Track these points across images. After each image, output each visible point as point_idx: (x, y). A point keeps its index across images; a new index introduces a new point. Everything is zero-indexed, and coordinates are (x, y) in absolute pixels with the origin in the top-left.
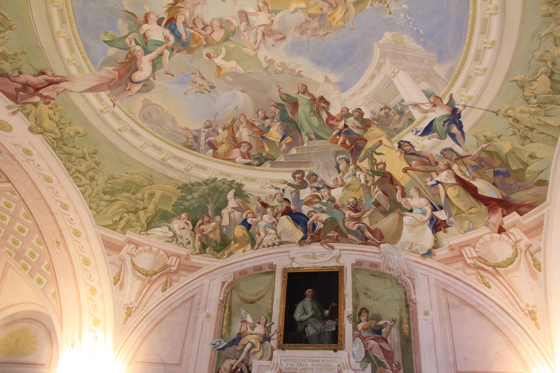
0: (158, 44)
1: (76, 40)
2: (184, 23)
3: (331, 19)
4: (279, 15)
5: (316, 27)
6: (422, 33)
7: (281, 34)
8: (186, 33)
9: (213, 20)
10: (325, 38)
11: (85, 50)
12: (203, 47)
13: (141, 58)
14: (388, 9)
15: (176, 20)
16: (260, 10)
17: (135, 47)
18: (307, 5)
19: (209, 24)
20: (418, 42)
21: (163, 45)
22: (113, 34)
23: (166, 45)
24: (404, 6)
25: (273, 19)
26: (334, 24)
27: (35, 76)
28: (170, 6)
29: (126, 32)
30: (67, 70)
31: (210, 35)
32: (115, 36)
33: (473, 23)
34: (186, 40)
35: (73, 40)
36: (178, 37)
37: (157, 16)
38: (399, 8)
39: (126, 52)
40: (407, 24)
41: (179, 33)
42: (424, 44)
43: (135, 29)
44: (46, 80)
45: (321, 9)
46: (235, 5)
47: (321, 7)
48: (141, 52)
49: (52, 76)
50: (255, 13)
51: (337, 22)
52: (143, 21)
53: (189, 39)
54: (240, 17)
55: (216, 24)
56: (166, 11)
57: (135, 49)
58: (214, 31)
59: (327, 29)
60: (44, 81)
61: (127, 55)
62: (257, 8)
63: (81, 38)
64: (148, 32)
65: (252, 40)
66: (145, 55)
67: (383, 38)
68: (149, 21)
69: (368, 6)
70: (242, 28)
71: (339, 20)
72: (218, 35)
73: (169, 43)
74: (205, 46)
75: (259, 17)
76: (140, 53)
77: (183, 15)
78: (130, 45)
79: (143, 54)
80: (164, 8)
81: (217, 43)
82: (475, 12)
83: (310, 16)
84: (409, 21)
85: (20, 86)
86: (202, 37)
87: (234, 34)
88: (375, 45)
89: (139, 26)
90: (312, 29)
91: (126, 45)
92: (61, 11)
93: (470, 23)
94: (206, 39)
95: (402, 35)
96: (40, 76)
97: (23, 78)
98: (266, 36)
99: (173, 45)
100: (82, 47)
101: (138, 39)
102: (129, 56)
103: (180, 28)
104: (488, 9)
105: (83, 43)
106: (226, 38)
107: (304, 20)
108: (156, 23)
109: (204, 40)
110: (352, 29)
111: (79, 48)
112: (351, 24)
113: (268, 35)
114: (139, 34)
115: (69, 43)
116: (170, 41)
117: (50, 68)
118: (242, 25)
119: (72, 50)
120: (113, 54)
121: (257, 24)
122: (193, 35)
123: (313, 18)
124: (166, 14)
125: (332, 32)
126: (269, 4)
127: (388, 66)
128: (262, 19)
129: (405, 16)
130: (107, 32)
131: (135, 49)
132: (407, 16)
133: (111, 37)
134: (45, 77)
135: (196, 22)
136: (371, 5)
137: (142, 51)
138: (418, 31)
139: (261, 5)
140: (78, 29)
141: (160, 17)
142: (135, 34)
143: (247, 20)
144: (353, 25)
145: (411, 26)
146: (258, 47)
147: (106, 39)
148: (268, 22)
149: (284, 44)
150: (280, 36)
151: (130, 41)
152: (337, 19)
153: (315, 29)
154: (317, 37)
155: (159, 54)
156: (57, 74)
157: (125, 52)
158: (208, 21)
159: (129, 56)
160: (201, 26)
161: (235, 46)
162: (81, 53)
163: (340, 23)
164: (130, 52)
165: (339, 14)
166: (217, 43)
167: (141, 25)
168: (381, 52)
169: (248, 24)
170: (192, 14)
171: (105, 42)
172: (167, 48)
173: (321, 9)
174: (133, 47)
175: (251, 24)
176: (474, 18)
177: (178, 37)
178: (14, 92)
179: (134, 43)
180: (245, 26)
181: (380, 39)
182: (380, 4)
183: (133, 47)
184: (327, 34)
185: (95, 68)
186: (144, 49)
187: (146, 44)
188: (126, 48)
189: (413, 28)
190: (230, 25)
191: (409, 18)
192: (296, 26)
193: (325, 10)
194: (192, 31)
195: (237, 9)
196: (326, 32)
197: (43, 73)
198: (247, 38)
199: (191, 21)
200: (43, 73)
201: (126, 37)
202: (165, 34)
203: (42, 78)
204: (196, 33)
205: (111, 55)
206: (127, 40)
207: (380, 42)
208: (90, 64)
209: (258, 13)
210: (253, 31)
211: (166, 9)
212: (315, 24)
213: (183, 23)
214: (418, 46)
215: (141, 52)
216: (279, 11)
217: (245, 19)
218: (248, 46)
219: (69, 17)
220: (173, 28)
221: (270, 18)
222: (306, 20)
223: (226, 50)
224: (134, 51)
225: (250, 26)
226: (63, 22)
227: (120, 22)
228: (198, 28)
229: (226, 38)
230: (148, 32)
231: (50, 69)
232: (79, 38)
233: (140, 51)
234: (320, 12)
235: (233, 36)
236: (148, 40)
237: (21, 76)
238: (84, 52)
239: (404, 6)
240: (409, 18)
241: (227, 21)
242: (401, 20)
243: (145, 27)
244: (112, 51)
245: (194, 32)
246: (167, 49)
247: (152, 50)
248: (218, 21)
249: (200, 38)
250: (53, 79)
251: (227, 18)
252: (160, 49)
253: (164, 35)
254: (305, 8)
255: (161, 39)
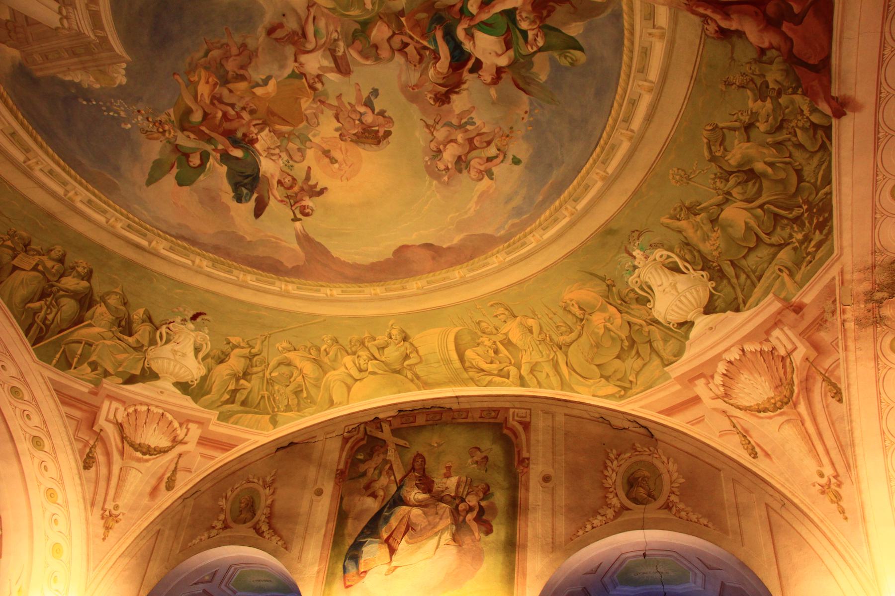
0: (487, 27)
1: (630, 67)
2: (437, 58)
3: (210, 80)
4: (288, 71)
5: (227, 61)
6: (80, 100)
7: (276, 40)
8: (435, 40)
9: (391, 58)
10: (205, 47)
11: (623, 44)
12: (406, 12)
13: (524, 4)
14: (146, 116)
15: (451, 66)
16: (319, 76)
17: (530, 27)
18: (254, 93)
19: (396, 53)
20: (78, 86)
21: (478, 24)
22: (563, 59)
23: (473, 23)
24: (129, 126)
25: (297, 64)
26: (203, 73)
27: (740, 34)
28: (457, 90)
29: (538, 59)
30: (674, 20)
31: (394, 34)
32: (560, 55)
33: (36, 140)
34: (435, 28)
35: (633, 69)
36: (450, 37)
37: (479, 76)
38: (133, 122)
39: (549, 22)
40: (108, 104)
41: (448, 43)
42: (63, 84)
43: (522, 60)
44: (727, 16)
45: (231, 91)
46: (358, 84)
47: (232, 94)
48: (521, 16)
49: (711, 19)
50: (325, 72)
51: (200, 79)
52: (504, 72)
53: (430, 29)
54: (348, 65)
55: (384, 53)
56: (464, 83)
57: (530, 24)
58: (389, 40)
59: (209, 63)
60: (732, 16)
61: (548, 15)
62: (324, 80)
63: (620, 68)
64: (500, 52)
65: (322, 23)
66: (515, 9)
67: (123, 72)
68: (494, 70)
69: (171, 111)
70: (341, 44)
71: (199, 82)
72: (380, 32)
73: (466, 26)
74: (402, 13)
75: (318, 66)
76: (524, 15)
77: (439, 73)
78: (539, 34)
79: (517, 12)
80: (467, 89)
81: (381, 18)
82: (47, 153)
83: (242, 78)
84: (109, 110)
85: (786, 27)
86: (408, 31)
87: (353, 34)
88: (128, 58)
89: (512, 65)
90: (231, 56)
91: (545, 35)
92: (628, 120)
93: (39, 139)
94: (400, 26)
95: (104, 86)
96: (733, 28)
97: (768, 39)
98: (300, 33)
99: (459, 21)
100: (626, 50)
101: (521, 41)
102: (545, 13)
103: (444, 51)
104: (37, 163)
105: (621, 59)
106: (365, 26)
107: (249, 70)
108: (484, 66)
109: (404, 26)
110: (174, 74)
111: (632, 51)
112: (181, 81)
113: (298, 35)
114: (517, 52)
115: (644, 67)
116: (465, 29)
117: (703, 36)
118: (342, 50)
119: (646, 53)
120: (574, 24)
121: (318, 54)
122: (424, 36)
123: (237, 74)
124: (466, 78)
125: (200, 59)
126: (308, 88)
127: (84, 28)
128: (314, 63)
129: (119, 114)
130: (571, 64)
131: (530, 24)
132: (116, 115)
133: (568, 54)
134: (724, 24)
135: (418, 57)
136: (169, 115)
137: (518, 18)
138: (88, 100)
139: (319, 86)
140: (617, 84)
141: (475, 75)
142: (524, 53)
143: (335, 59)
144: (177, 80)
145: (101, 103)
146: (309, 10)
147: (578, 53)
148: (303, 58)
149: (269, 18)
150: (279, 34)
151: (535, 40)
152: (203, 81)
153: (227, 58)
154: (219, 45)
155: (489, 6)
156: (697, 20)
157: (549, 22)
158: (399, 58)
159: (545, 13)
160: (410, 49)
161: (348, 11)
162: (632, 43)
163: (196, 78)
164: (542, 19)
165: (204, 90)
166: (381, 18)
167: (509, 66)
168: (111, 49)
169: (333, 52)
170: (424, 71)
171: (581, 49)
172: (472, 17)
173: (231, 91)
174: (533, 29)
175: (328, 53)
176: (41, 147)
177: (450, 37)
178: (810, 20)
179: (531, 34)
180: (337, 49)
181: (125, 69)
182: (159, 119)
183: (533, 29)
184: (206, 55)
185: (621, 7)
186: (514, 22)
187: (508, 29)
188: (547, 29)
189: (97, 102)
190: (362, 51)
191: (111, 114)
192: (257, 56)
193: (225, 92)
194: (425, 43)
195: (353, 78)
196: (209, 55)
197: (724, 34)
198: (331, 28)
199: (426, 60)
200: (724, 34)
201: (540, 50)
202: (472, 42)
203: (733, 25)
204: (418, 39)
205: (578, 23)
206: (540, 43)
207: (124, 65)
208: (625, 16)
209: (321, 73)
210: (323, 41)
211: (464, 86)
212: (231, 66)
213: (439, 59)
214: (68, 78)
215: (521, 16)
216: (290, 77)
217: (339, 61)
218: (326, 10)
219: (621, 106)
220: (457, 53)
221: (301, 64)
222: (247, 70)
223: (365, 4)
224: (534, 22)
225: (329, 50)
226: (633, 103)
227: (543, 77)
228: (415, 48)
229: (365, 26)
230: (500, 52)
231: (706, 35)
232: (624, 67)
233: (523, 19)
234: (231, 86)
235: (356, 31)
236: (503, 37)
237: (766, 45)
238: (626, 42)
239: (129, 126)
240: (111, 114)
241: (367, 58)
242: (119, 107)
243: (503, 61)
244: (575, 30)
245: (421, 41)
246: (471, 13)
247: (500, 16)
248: (382, 57)
249: (411, 30)
250: (713, 12)
251: (368, 63)
252: (485, 17)
253: (474, 43)
254: (253, 87)
255: (480, 36)
